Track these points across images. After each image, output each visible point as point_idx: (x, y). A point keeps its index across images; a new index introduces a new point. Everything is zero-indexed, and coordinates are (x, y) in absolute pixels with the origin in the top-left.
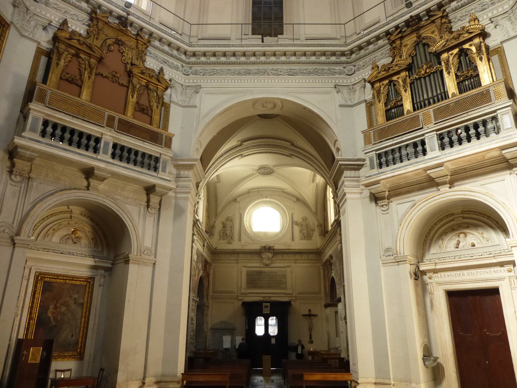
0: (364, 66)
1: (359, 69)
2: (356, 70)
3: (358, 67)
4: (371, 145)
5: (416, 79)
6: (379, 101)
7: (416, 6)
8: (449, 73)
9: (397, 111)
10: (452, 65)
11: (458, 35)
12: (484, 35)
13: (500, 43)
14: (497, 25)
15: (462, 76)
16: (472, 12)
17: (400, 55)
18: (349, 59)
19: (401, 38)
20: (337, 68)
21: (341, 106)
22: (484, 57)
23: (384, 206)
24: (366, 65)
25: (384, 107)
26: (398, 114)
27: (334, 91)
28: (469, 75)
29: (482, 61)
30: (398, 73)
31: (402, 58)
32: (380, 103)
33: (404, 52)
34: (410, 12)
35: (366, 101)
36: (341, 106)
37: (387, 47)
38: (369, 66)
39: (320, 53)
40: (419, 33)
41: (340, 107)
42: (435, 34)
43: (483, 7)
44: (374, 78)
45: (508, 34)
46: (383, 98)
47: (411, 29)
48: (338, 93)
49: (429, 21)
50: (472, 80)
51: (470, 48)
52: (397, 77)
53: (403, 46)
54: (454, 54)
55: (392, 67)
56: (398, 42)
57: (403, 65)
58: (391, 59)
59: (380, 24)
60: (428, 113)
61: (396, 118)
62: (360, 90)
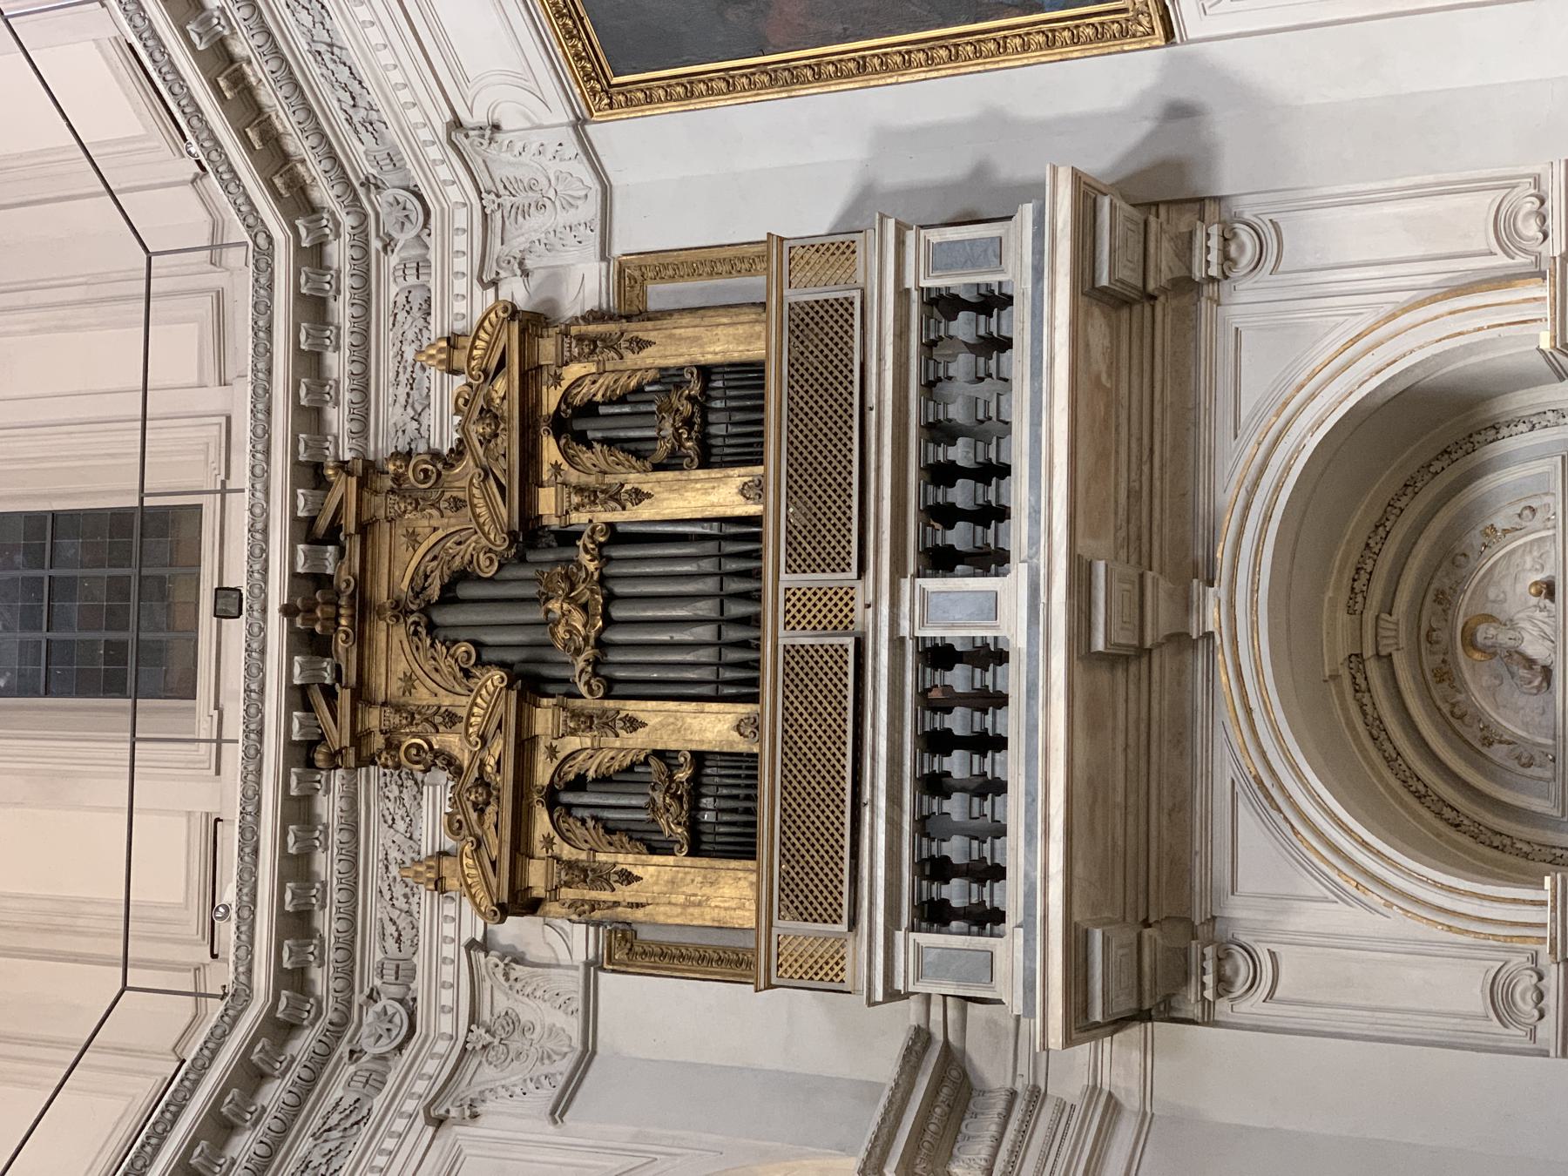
0: (398, 940)
1: (404, 973)
2: (395, 990)
3: (390, 975)
4: (851, 941)
5: (596, 663)
6: (628, 878)
7: (251, 573)
8: (639, 496)
9: (716, 797)
10: (609, 479)
11: (481, 418)
12: (532, 323)
13: (604, 265)
14: (521, 264)
15: (677, 436)
16: (409, 354)
17: (438, 719)
18: (319, 1014)
19: (362, 695)
20: (338, 1089)
21: (558, 1111)
22: (635, 329)
23: (1228, 970)
24: (403, 922)
25: (670, 860)
26: (735, 792)
27: (457, 1133)
28: (686, 408)
29: (649, 343)
30: (525, 746)
31: (463, 713)
32: (638, 879)
33: (434, 701)
34: (264, 610)
35: (593, 966)
36: (558, 1111)
37: (367, 790)
38: (414, 908)
39: (203, 1143)
40: (382, 606)
41: (561, 1116)
42: (428, 530)
43: (415, 308)
44: (493, 881)
45: (582, 227)
46: (620, 858)
47: (342, 636)
48: (475, 1116)
49: (354, 547)
50: (718, 404)
51: (565, 384)
52: (541, 757)
53: (407, 698)
54: (561, 460)
55: (482, 765)
56: (373, 719)
57: (501, 708)
58: (442, 776)
59: (233, 814)
60: (794, 599)
61: (751, 812)
62: (518, 986)
